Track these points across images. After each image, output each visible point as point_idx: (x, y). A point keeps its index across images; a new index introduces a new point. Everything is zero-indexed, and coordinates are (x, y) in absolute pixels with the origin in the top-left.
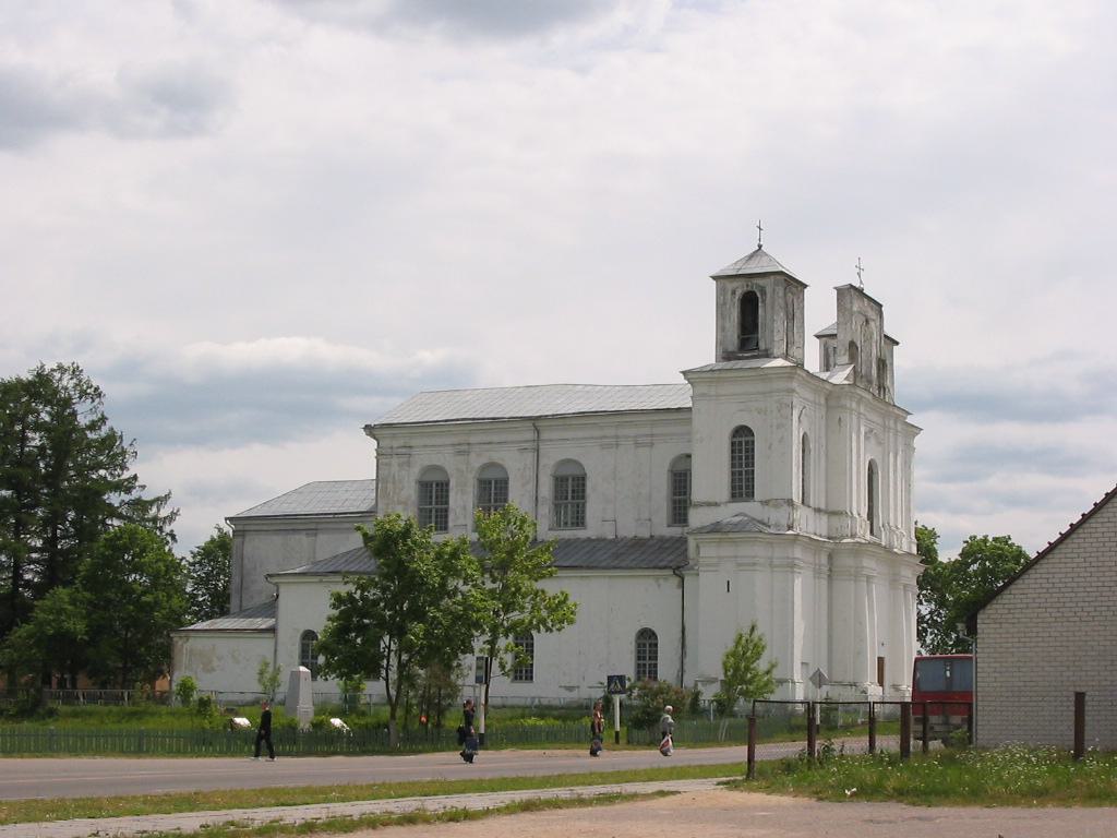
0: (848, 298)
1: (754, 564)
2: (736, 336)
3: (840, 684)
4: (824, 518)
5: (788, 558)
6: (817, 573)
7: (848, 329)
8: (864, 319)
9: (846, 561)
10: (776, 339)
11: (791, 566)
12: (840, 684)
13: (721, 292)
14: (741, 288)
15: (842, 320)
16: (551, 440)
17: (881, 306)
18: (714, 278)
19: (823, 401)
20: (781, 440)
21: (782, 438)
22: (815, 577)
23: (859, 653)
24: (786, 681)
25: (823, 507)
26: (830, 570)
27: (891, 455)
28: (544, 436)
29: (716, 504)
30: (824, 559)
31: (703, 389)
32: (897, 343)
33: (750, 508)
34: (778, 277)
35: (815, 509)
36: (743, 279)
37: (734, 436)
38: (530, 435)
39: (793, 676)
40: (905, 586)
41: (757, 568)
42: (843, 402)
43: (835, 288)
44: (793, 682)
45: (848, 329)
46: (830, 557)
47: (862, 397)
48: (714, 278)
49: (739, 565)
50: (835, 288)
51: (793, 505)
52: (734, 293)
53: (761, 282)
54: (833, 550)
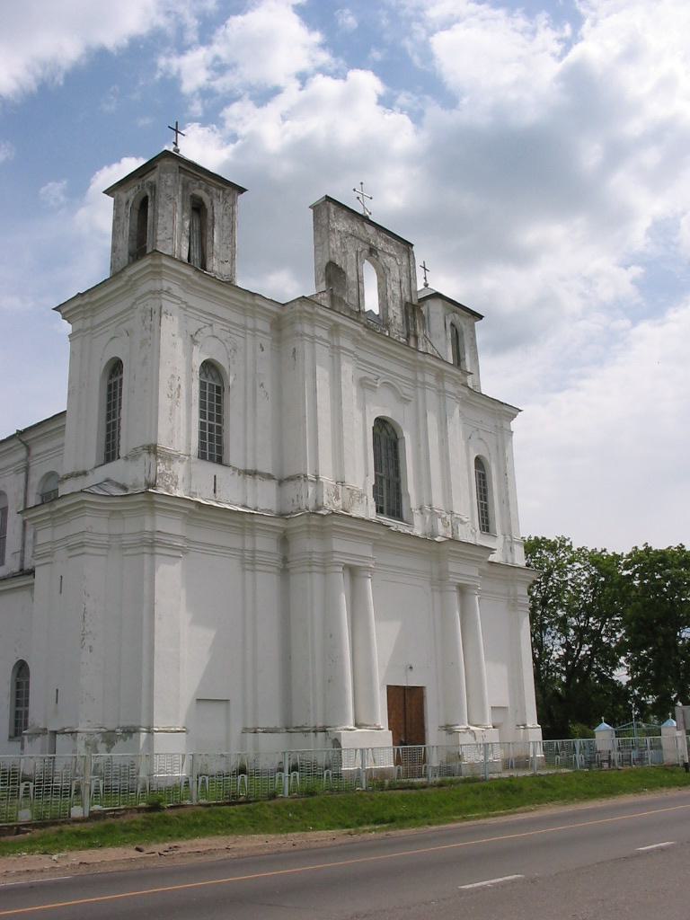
0: (324, 213)
1: (82, 545)
2: (126, 252)
3: (302, 730)
4: (271, 486)
5: (142, 532)
6: (249, 562)
7: (326, 249)
8: (367, 247)
9: (307, 545)
10: (159, 238)
11: (151, 544)
12: (302, 730)
13: (117, 205)
14: (130, 195)
15: (319, 240)
16: (38, 455)
17: (412, 245)
18: (108, 192)
19: (263, 325)
20: (144, 363)
21: (145, 358)
22: (244, 570)
23: (329, 681)
24: (130, 732)
25: (266, 466)
26: (285, 560)
27: (432, 421)
28: (34, 451)
29: (85, 473)
30: (266, 544)
31: (79, 324)
32: (481, 317)
33: (116, 470)
34: (166, 163)
35: (246, 472)
36: (133, 182)
37: (111, 377)
38: (22, 454)
39: (151, 718)
40: (463, 590)
41: (86, 549)
42: (298, 328)
43: (310, 207)
44: (150, 731)
45: (326, 249)
46: (284, 540)
47: (337, 325)
48: (108, 192)
49: (70, 548)
50: (310, 207)
51: (155, 452)
52: (127, 203)
53: (152, 177)
54: (285, 531)
